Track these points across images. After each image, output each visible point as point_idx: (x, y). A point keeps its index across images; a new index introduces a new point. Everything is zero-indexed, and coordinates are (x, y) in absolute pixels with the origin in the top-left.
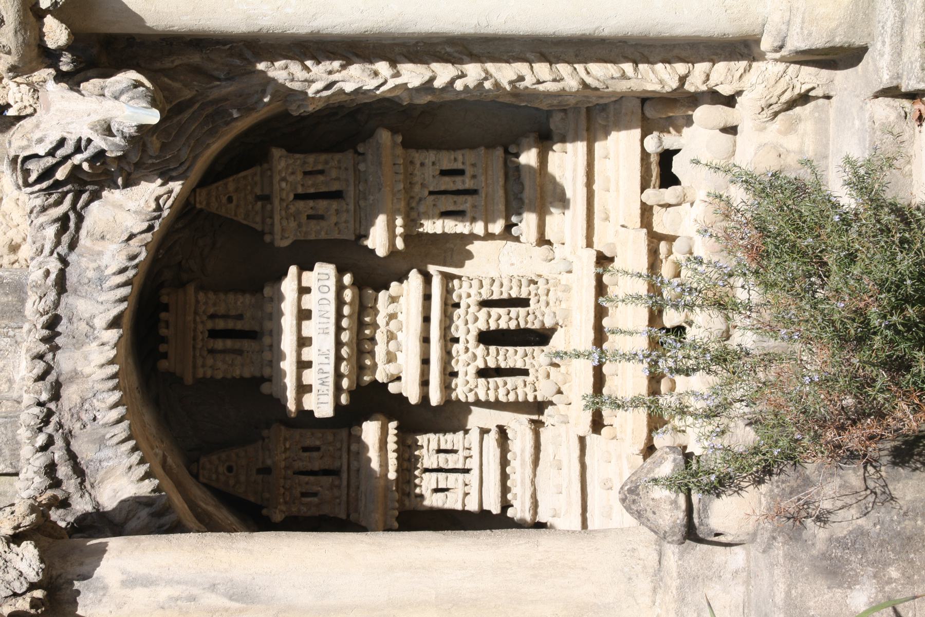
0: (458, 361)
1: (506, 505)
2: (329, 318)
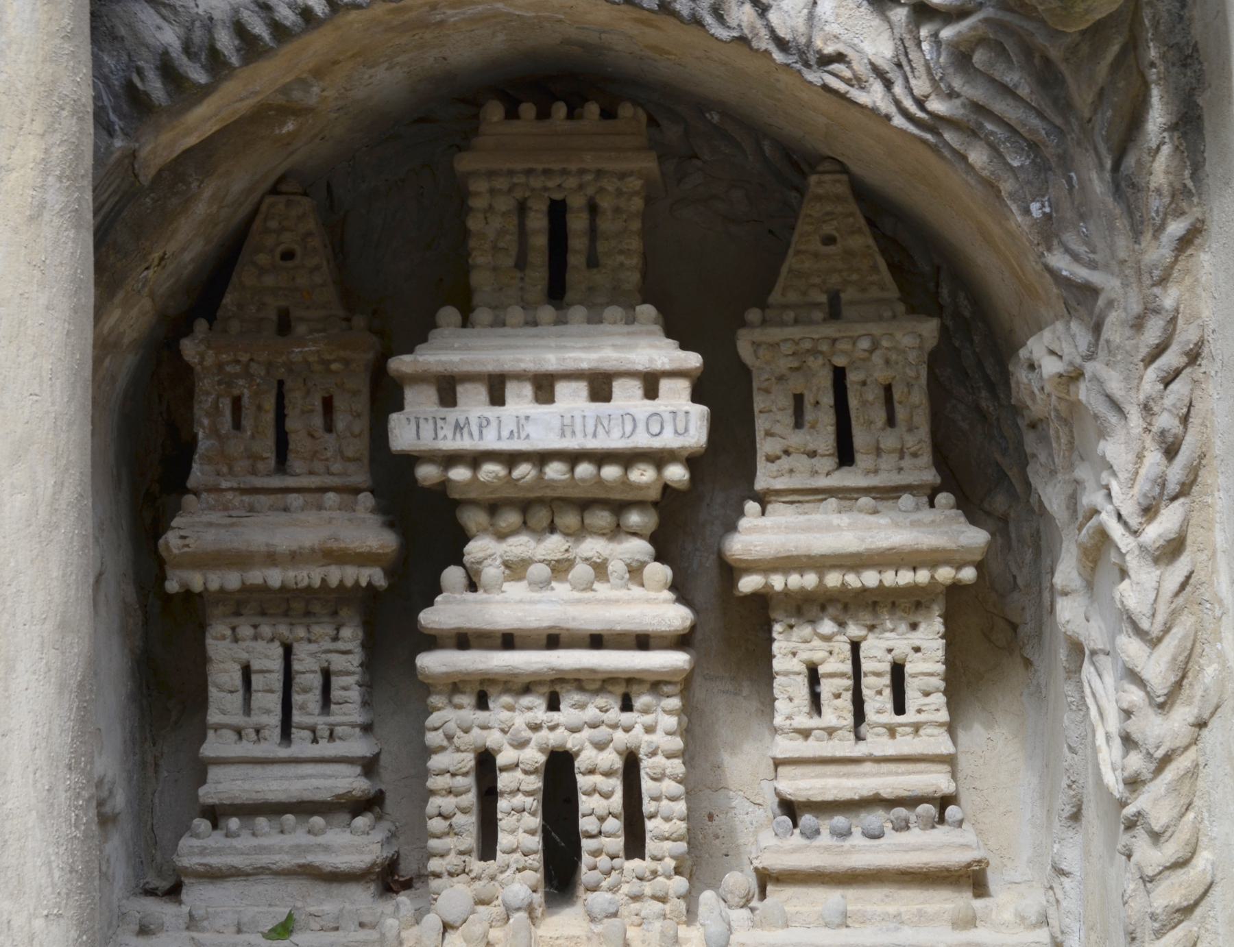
0: (511, 708)
1: (215, 815)
2: (595, 435)
